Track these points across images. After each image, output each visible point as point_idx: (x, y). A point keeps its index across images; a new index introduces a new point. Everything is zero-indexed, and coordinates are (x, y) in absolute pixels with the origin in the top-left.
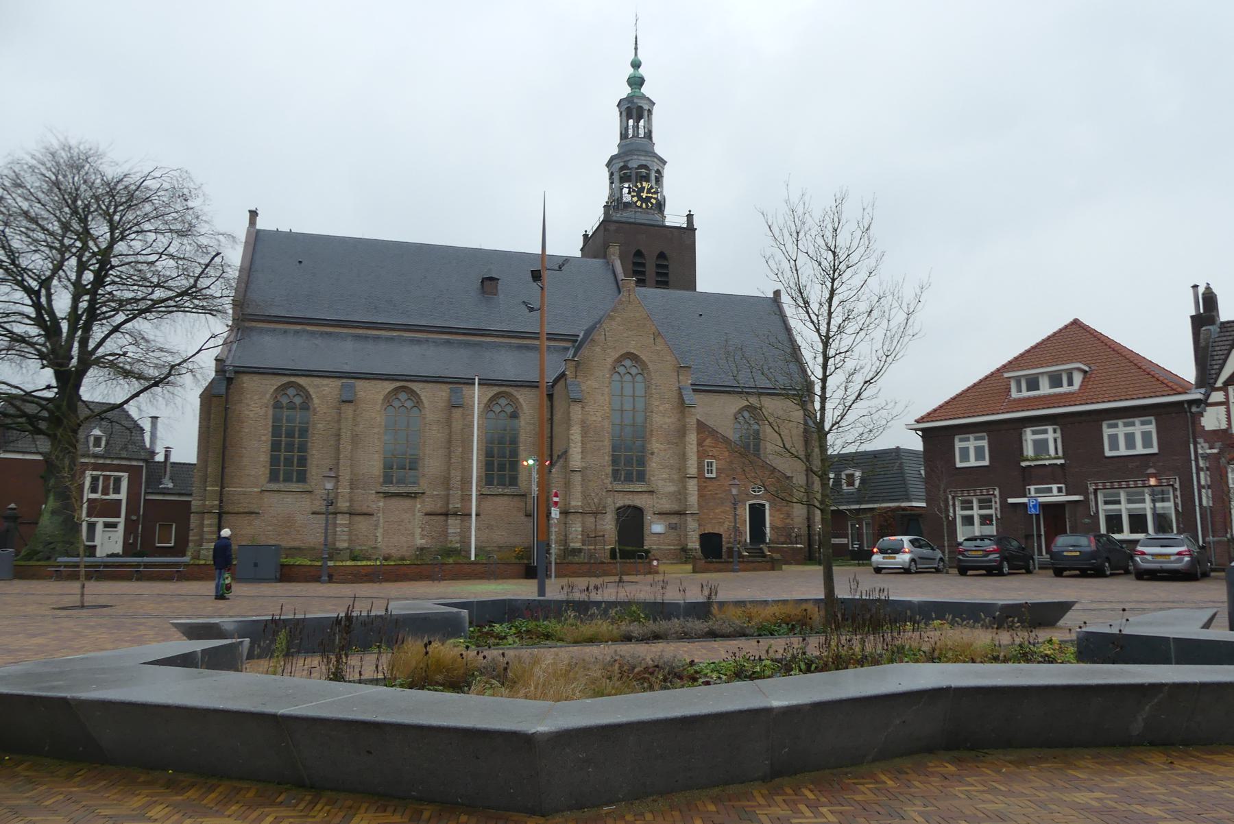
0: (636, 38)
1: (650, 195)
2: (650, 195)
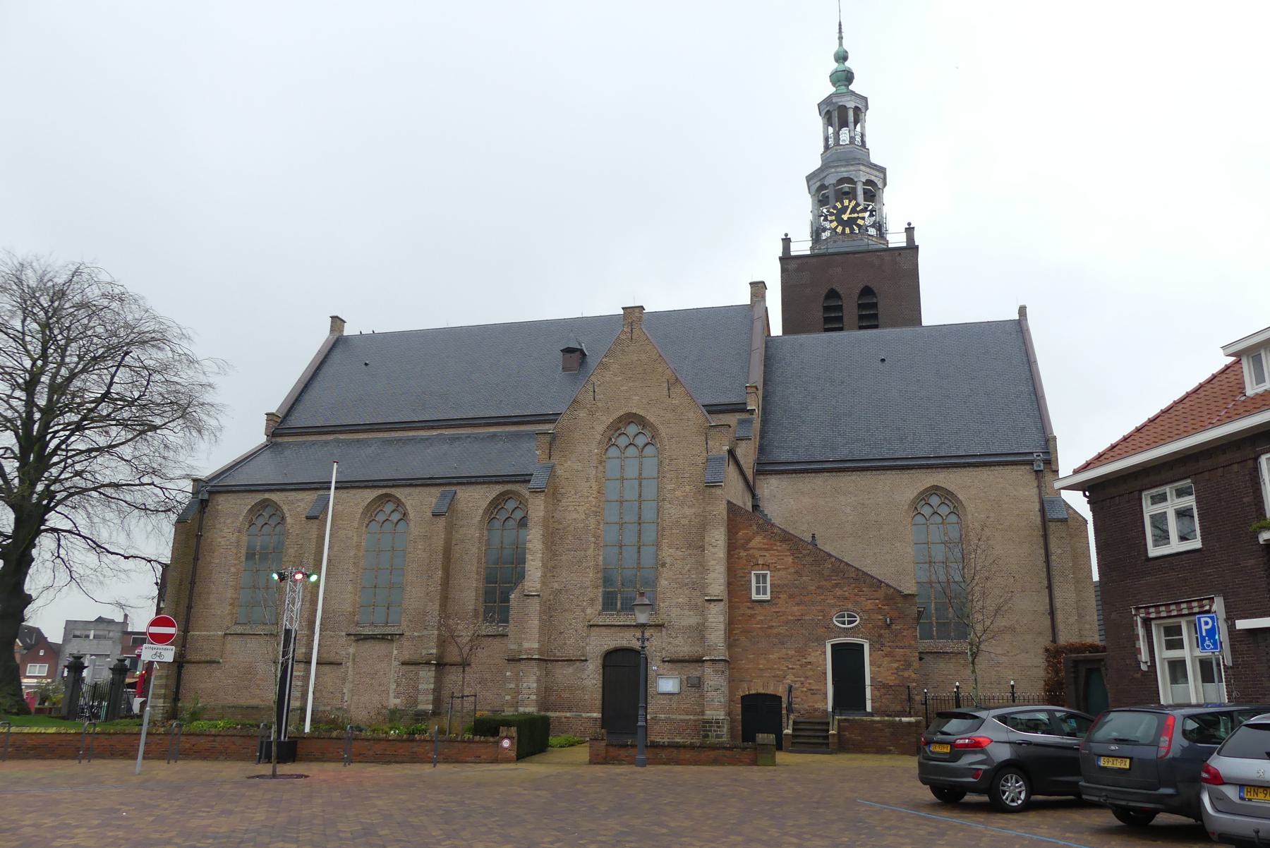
0: (840, 25)
1: (856, 215)
2: (856, 215)
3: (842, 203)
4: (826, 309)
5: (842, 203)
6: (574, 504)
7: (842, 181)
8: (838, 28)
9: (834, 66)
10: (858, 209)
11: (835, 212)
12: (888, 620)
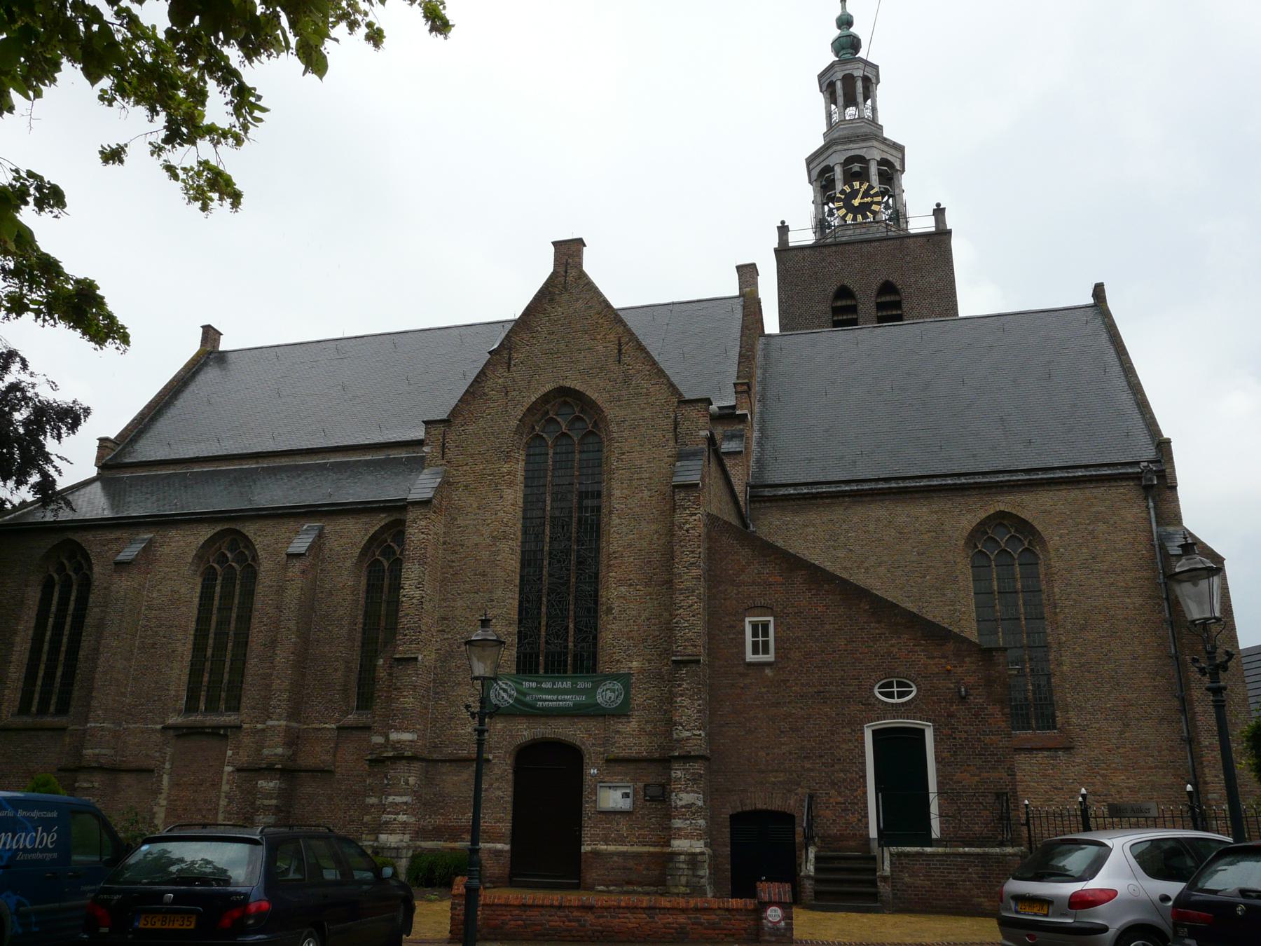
1: (869, 199)
2: (869, 199)
3: (851, 186)
4: (836, 311)
5: (851, 186)
6: (475, 522)
7: (850, 160)
9: (836, 32)
10: (872, 192)
11: (843, 197)
12: (963, 690)
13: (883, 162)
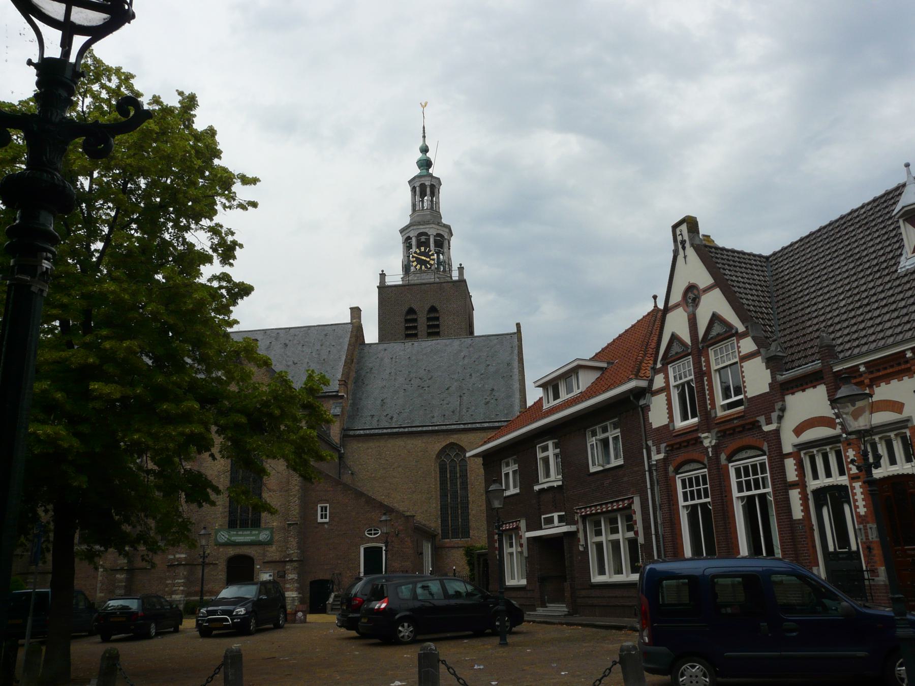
0: (424, 128)
3: (420, 250)
4: (407, 321)
5: (420, 250)
8: (422, 129)
13: (438, 235)
